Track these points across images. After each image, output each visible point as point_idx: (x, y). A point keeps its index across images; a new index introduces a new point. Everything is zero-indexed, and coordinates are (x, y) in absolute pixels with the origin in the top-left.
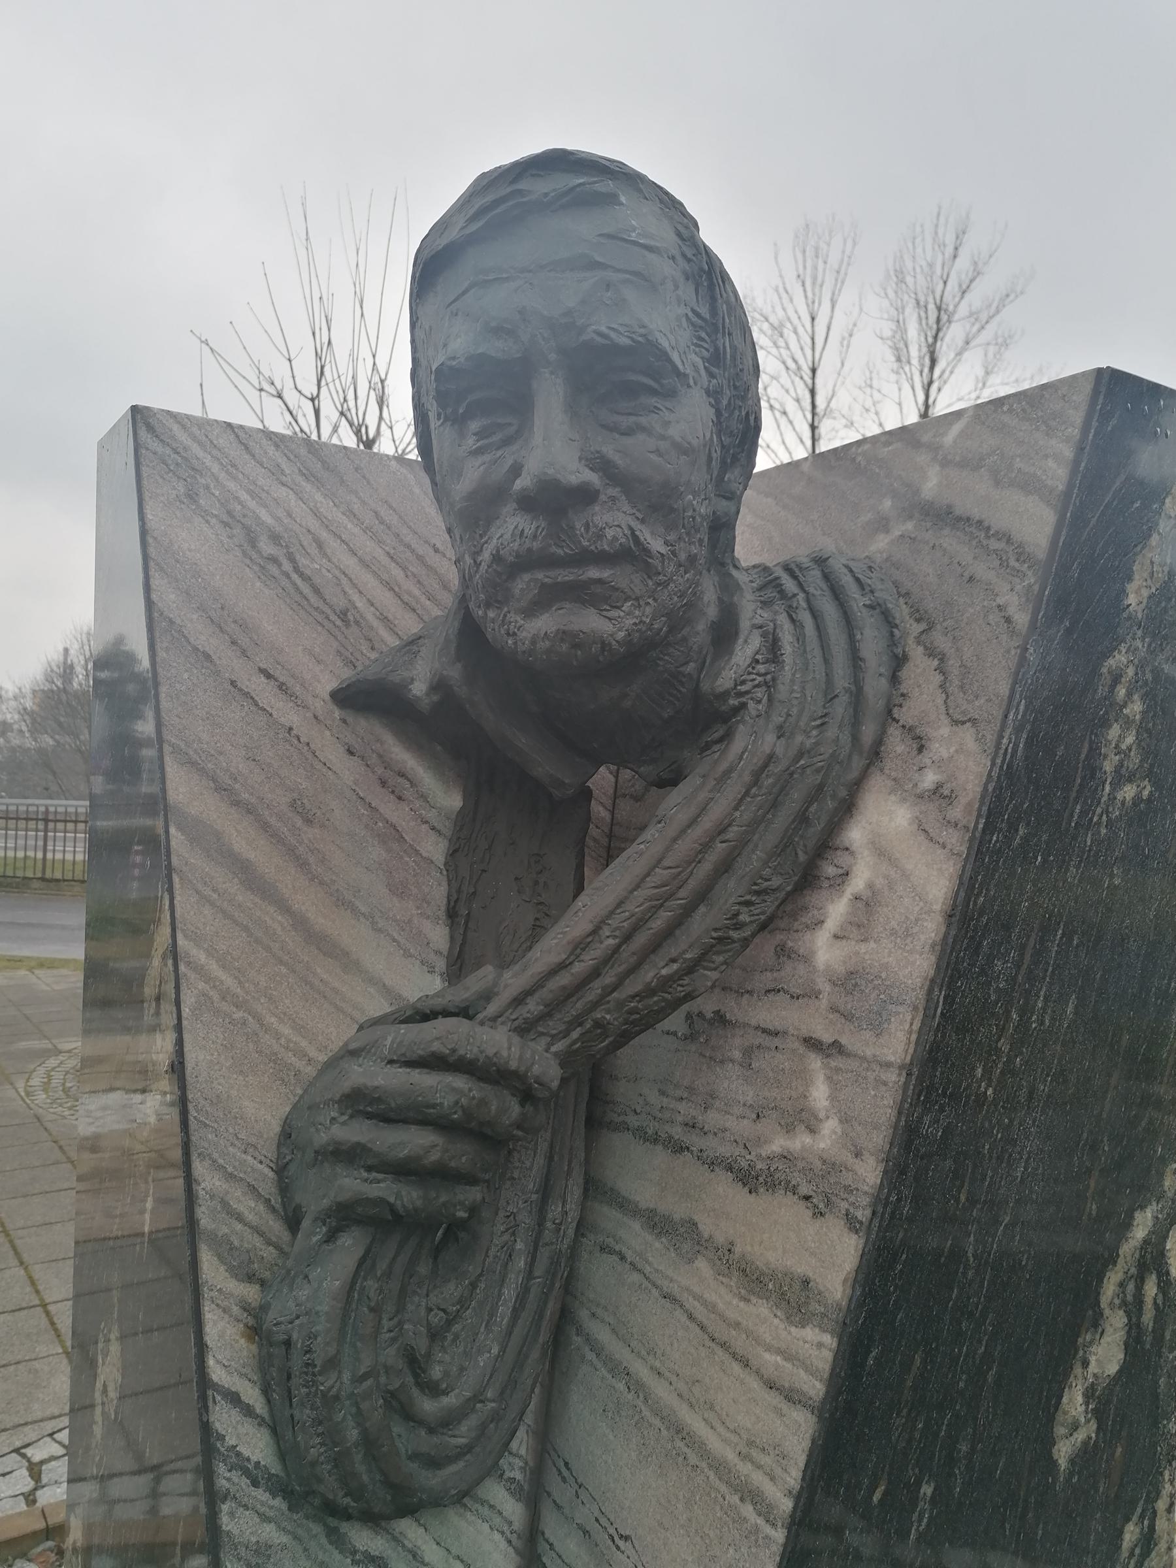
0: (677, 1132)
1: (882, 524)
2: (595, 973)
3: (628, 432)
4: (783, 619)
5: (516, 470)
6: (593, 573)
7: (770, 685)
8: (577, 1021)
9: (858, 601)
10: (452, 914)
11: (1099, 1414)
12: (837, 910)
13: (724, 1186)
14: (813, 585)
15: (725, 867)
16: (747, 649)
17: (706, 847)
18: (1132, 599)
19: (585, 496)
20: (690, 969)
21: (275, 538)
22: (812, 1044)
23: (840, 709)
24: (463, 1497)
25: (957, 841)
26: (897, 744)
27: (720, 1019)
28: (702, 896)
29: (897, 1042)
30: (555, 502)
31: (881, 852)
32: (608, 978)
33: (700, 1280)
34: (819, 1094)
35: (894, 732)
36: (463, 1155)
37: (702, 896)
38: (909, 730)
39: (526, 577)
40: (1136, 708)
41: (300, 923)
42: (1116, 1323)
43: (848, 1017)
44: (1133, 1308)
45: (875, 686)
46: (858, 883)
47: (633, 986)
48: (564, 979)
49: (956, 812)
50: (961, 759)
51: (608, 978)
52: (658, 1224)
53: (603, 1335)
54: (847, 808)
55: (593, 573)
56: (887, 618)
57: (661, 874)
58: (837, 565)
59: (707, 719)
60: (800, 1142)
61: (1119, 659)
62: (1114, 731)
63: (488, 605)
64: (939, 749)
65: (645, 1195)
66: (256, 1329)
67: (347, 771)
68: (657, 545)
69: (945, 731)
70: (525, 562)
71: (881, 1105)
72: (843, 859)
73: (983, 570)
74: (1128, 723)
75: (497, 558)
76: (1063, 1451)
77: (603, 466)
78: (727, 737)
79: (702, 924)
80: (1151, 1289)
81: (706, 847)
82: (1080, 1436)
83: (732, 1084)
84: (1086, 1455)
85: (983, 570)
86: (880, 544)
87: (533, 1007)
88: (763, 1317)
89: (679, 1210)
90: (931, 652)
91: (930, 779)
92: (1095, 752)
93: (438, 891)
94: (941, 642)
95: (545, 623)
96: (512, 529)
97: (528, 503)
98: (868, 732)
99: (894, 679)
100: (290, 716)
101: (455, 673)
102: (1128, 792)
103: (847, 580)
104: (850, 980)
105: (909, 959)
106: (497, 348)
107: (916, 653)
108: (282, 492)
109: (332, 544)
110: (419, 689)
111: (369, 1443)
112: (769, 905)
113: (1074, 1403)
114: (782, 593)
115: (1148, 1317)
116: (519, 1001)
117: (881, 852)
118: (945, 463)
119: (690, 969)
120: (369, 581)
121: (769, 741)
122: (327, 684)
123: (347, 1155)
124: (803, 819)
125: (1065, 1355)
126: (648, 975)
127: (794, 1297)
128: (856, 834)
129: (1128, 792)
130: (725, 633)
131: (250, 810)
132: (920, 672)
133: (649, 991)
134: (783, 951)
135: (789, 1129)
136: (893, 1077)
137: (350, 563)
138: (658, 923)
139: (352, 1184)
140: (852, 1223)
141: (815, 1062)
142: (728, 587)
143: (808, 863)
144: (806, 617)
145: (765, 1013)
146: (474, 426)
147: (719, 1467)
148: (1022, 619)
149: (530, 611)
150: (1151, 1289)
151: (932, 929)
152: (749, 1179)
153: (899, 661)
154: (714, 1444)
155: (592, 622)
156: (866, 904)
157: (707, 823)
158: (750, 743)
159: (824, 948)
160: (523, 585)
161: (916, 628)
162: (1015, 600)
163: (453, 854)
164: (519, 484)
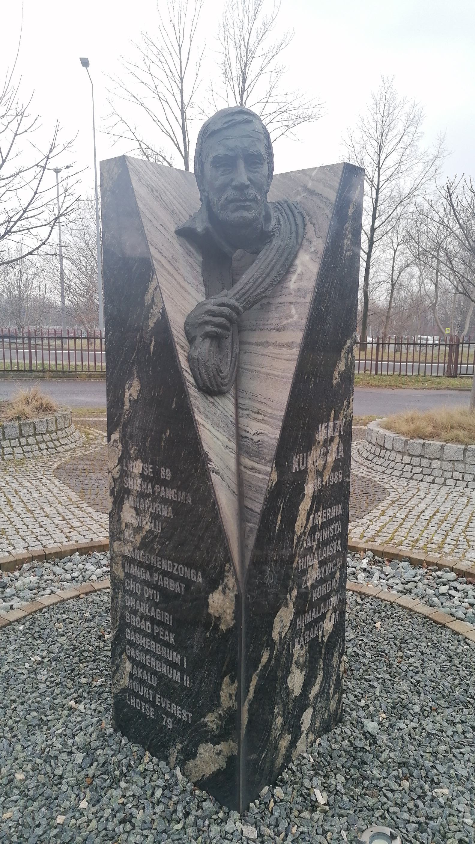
0: (261, 327)
1: (298, 193)
2: (249, 290)
3: (255, 173)
4: (280, 215)
5: (232, 180)
6: (248, 203)
7: (279, 230)
8: (245, 300)
9: (296, 212)
10: (205, 285)
11: (340, 377)
12: (294, 277)
13: (274, 333)
14: (287, 208)
15: (272, 269)
16: (274, 222)
17: (269, 264)
18: (350, 213)
19: (248, 187)
20: (266, 290)
21: (157, 191)
22: (291, 303)
23: (294, 235)
24: (228, 392)
25: (319, 261)
26: (305, 243)
27: (269, 303)
28: (268, 275)
29: (309, 298)
30: (242, 188)
31: (303, 265)
32: (251, 291)
33: (271, 349)
34: (293, 311)
35: (305, 240)
36: (228, 324)
37: (268, 275)
38: (308, 240)
39: (233, 204)
40: (350, 236)
41: (179, 283)
42: (344, 360)
43: (299, 296)
44: (347, 359)
45: (301, 230)
46: (299, 271)
47: (255, 293)
48: (243, 291)
49: (318, 255)
50: (319, 244)
51: (251, 291)
52: (257, 344)
53: (248, 367)
54: (295, 257)
55: (248, 203)
56: (302, 215)
57: (261, 270)
58: (290, 202)
59: (265, 237)
60: (290, 320)
61: (347, 225)
62: (345, 241)
63: (221, 210)
64: (314, 243)
65: (254, 340)
66: (189, 359)
67: (180, 250)
68: (259, 198)
69: (316, 239)
70: (232, 201)
71: (306, 310)
72: (295, 267)
73: (322, 205)
74: (348, 239)
75: (226, 199)
76: (334, 382)
77: (250, 179)
78: (271, 241)
79: (268, 281)
80: (350, 356)
81: (269, 264)
82: (337, 380)
83: (274, 314)
84: (338, 384)
85: (322, 205)
86: (299, 198)
87: (237, 296)
88: (285, 351)
89: (263, 340)
90: (312, 223)
91: (313, 249)
92: (342, 244)
93: (202, 280)
94: (314, 221)
95: (237, 214)
96: (230, 193)
97: (235, 188)
98: (300, 240)
99: (304, 229)
100: (169, 237)
101: (209, 226)
102: (348, 254)
103: (293, 206)
104: (299, 290)
105: (310, 283)
106: (230, 153)
107: (309, 223)
108: (155, 178)
109: (167, 193)
110: (199, 230)
111: (214, 376)
112: (280, 278)
113: (336, 374)
114: (279, 209)
115: (349, 362)
116: (234, 295)
117: (303, 265)
118: (313, 180)
119: (266, 290)
120: (175, 202)
121: (280, 242)
122: (173, 230)
123: (206, 323)
124: (287, 259)
125: (334, 365)
126: (258, 291)
127: (290, 346)
128: (297, 262)
129: (348, 254)
130: (268, 218)
131: (165, 257)
132: (309, 226)
133: (258, 294)
134: (282, 287)
135: (287, 319)
136: (308, 304)
137: (171, 197)
138: (260, 280)
139: (209, 328)
140: (301, 330)
141: (292, 306)
142: (266, 206)
143: (288, 268)
144: (284, 214)
145: (280, 300)
146: (222, 169)
147: (277, 376)
148: (330, 216)
149: (232, 212)
150: (350, 356)
151: (315, 277)
152: (279, 330)
153: (305, 225)
154: (276, 373)
155: (246, 214)
156: (301, 275)
157: (269, 259)
158: (276, 242)
159: (293, 283)
160: (231, 206)
161: (308, 218)
162: (328, 212)
163: (203, 271)
164: (234, 183)
